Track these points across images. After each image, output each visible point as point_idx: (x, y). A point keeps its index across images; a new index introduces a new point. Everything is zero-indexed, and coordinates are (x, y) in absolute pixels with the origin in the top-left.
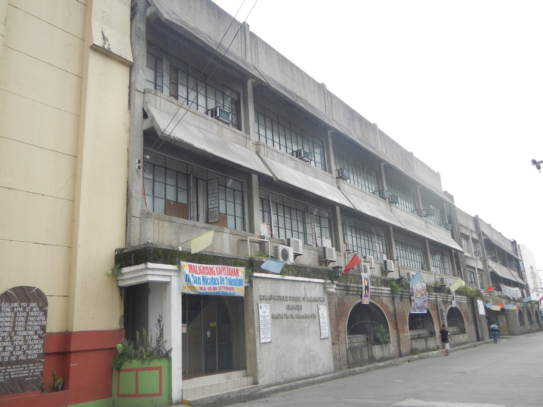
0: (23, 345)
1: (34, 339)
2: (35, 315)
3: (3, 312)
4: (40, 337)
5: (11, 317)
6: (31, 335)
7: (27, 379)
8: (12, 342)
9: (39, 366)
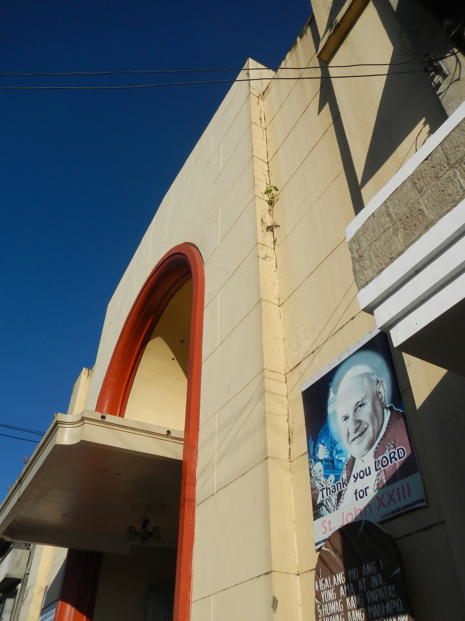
2: (379, 598)
3: (325, 602)
5: (339, 613)
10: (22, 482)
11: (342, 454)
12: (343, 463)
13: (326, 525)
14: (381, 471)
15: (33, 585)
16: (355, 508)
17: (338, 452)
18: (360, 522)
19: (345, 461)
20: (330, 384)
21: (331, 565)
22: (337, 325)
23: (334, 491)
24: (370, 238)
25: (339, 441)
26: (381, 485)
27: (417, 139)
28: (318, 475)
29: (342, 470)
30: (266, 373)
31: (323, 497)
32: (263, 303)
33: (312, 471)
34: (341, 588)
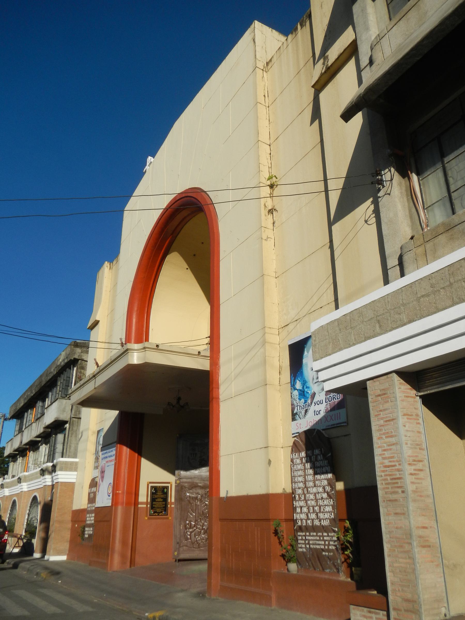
0: (315, 506)
1: (324, 499)
2: (320, 465)
3: (295, 464)
4: (330, 496)
5: (302, 470)
6: (321, 492)
7: (324, 553)
8: (306, 502)
9: (332, 537)
10: (96, 377)
11: (309, 389)
12: (309, 394)
13: (298, 425)
14: (328, 403)
15: (87, 429)
16: (314, 419)
17: (307, 387)
18: (315, 429)
19: (311, 393)
20: (305, 346)
21: (299, 448)
22: (312, 308)
23: (303, 408)
24: (320, 338)
25: (308, 382)
26: (327, 411)
27: (366, 211)
28: (296, 397)
29: (308, 398)
30: (267, 330)
31: (297, 410)
32: (265, 277)
33: (292, 394)
34: (304, 459)
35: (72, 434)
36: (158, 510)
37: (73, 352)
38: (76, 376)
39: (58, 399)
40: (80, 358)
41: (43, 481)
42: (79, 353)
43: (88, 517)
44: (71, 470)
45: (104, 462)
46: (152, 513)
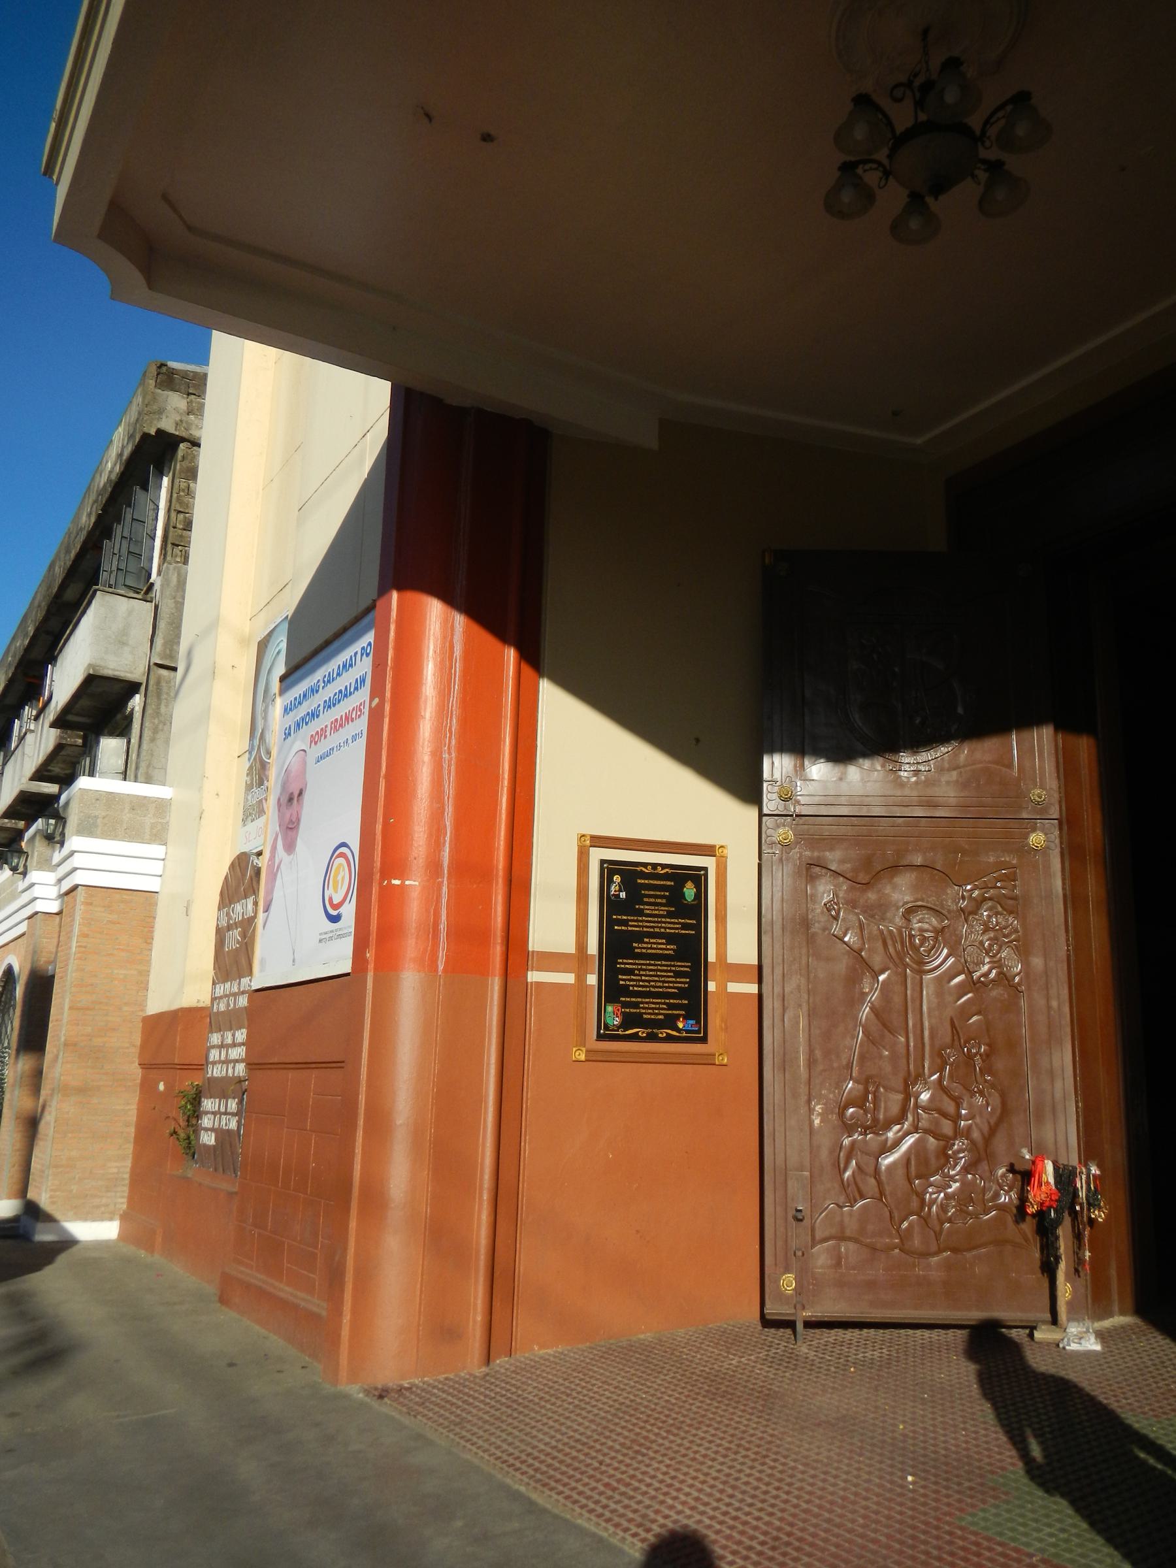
35: (155, 731)
36: (652, 1009)
37: (153, 409)
38: (169, 510)
39: (98, 592)
40: (184, 434)
41: (25, 898)
42: (181, 414)
43: (213, 1047)
44: (134, 834)
45: (299, 745)
46: (617, 1021)
